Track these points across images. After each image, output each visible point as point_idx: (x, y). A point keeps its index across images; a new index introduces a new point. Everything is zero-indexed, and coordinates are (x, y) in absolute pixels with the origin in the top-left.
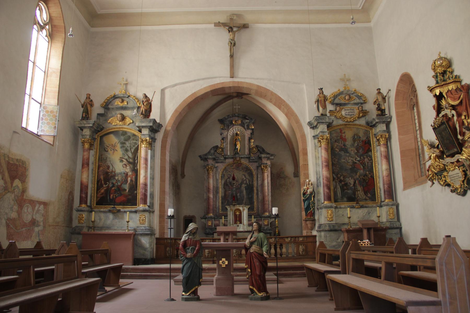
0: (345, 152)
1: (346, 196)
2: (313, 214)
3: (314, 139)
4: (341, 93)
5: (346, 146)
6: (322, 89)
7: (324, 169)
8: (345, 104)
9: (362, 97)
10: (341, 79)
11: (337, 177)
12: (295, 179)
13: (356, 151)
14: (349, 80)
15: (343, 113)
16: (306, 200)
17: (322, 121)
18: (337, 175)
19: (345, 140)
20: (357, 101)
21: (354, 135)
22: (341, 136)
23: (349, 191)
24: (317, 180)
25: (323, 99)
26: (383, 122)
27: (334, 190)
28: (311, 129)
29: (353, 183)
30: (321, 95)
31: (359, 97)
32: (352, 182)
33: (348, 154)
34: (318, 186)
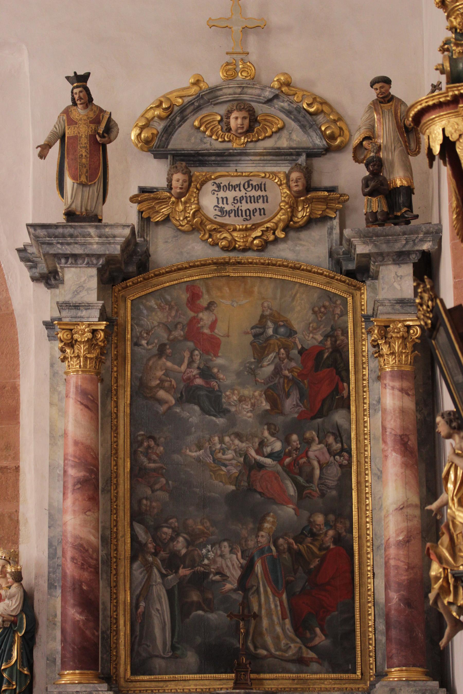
0: (205, 411)
1: (199, 640)
3: (52, 337)
4: (205, 98)
5: (214, 377)
6: (81, 80)
7: (70, 496)
8: (224, 157)
9: (320, 118)
10: (212, 24)
11: (155, 539)
13: (266, 406)
14: (259, 28)
15: (209, 201)
17: (68, 250)
18: (154, 531)
19: (212, 345)
20: (295, 137)
21: (263, 317)
22: (193, 322)
23: (217, 617)
25: (83, 131)
26: (400, 257)
27: (135, 606)
28: (41, 287)
29: (237, 573)
30: (80, 112)
31: (306, 120)
32: (232, 564)
33: (220, 421)
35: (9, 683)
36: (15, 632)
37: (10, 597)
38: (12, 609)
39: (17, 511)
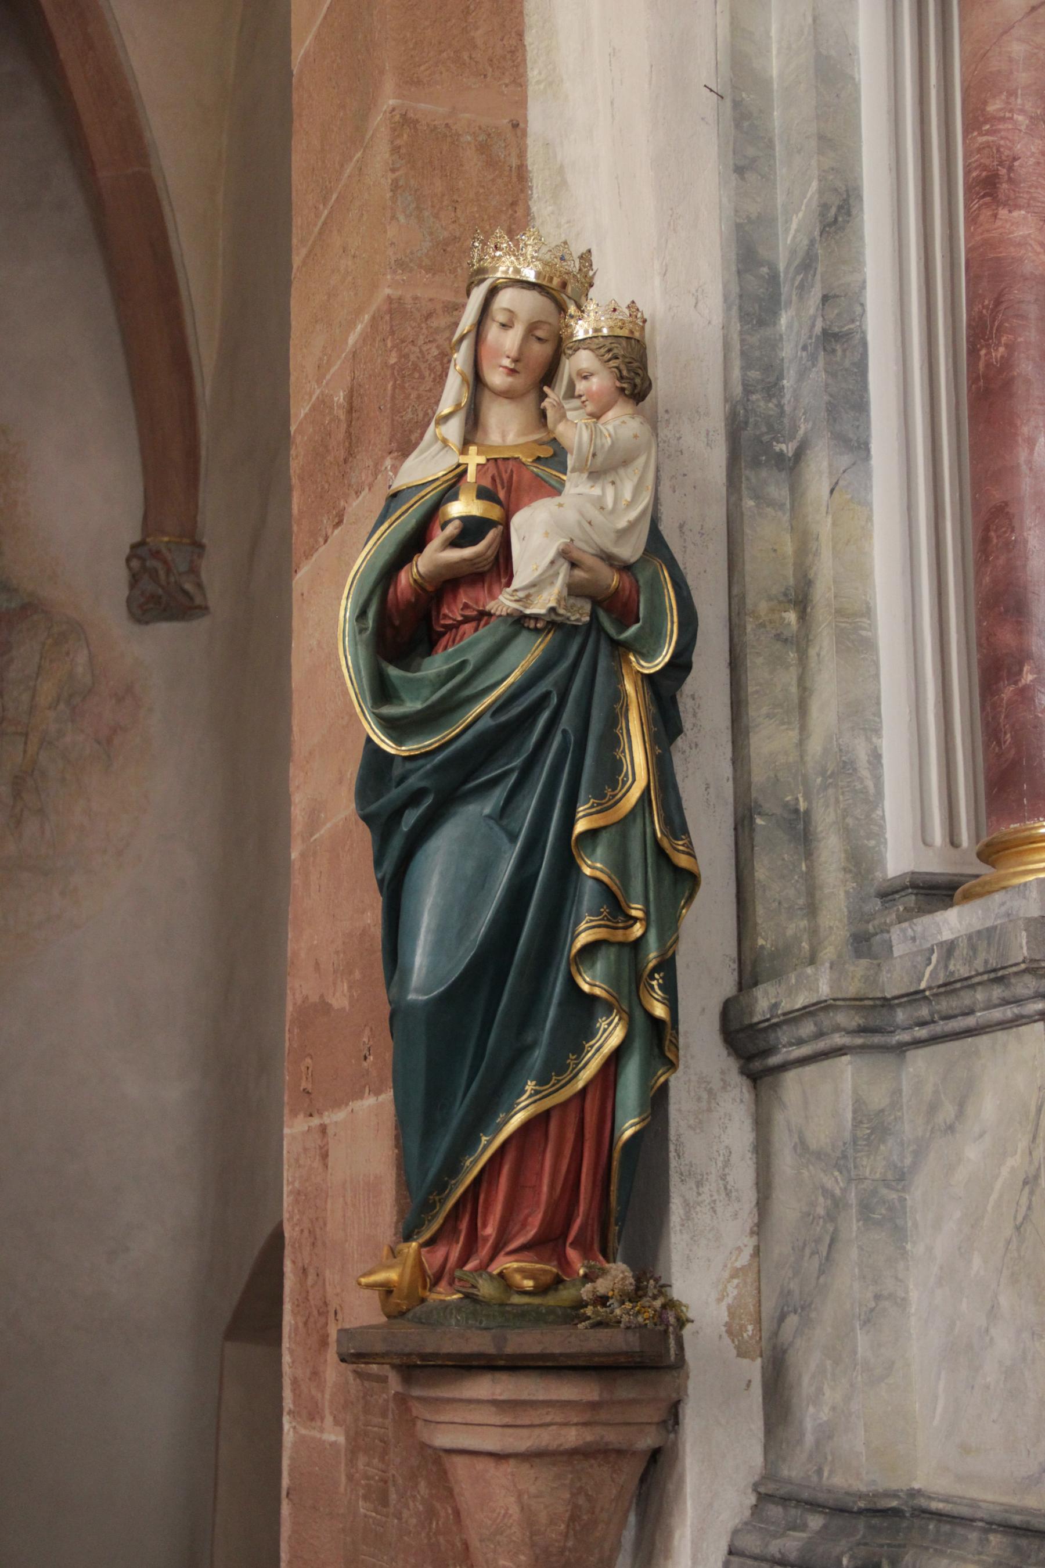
2: (617, 1195)
12: (149, 652)
16: (456, 779)
24: (756, 292)
34: (758, 448)
35: (614, 907)
36: (620, 649)
37: (600, 470)
38: (622, 524)
39: (518, 127)
